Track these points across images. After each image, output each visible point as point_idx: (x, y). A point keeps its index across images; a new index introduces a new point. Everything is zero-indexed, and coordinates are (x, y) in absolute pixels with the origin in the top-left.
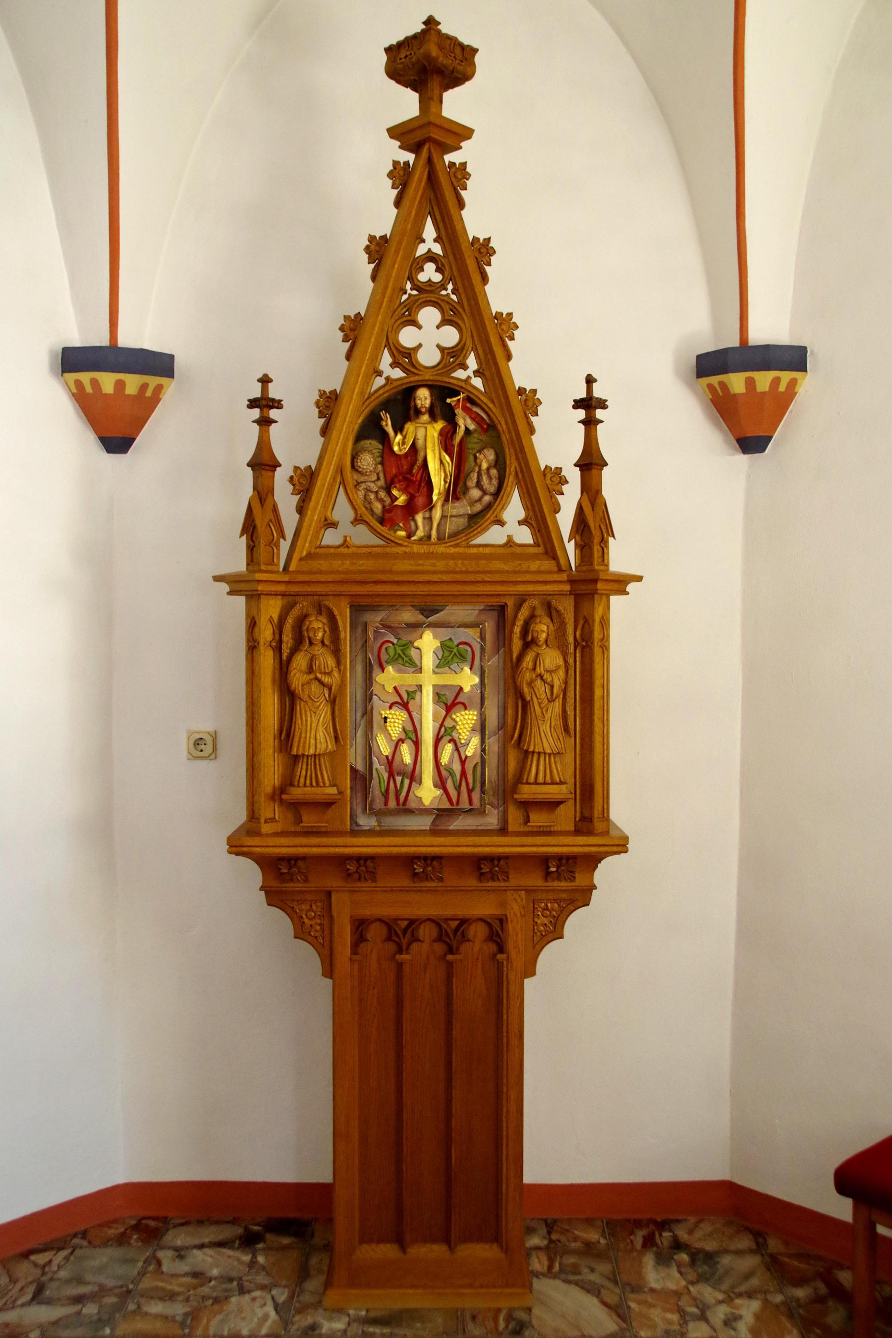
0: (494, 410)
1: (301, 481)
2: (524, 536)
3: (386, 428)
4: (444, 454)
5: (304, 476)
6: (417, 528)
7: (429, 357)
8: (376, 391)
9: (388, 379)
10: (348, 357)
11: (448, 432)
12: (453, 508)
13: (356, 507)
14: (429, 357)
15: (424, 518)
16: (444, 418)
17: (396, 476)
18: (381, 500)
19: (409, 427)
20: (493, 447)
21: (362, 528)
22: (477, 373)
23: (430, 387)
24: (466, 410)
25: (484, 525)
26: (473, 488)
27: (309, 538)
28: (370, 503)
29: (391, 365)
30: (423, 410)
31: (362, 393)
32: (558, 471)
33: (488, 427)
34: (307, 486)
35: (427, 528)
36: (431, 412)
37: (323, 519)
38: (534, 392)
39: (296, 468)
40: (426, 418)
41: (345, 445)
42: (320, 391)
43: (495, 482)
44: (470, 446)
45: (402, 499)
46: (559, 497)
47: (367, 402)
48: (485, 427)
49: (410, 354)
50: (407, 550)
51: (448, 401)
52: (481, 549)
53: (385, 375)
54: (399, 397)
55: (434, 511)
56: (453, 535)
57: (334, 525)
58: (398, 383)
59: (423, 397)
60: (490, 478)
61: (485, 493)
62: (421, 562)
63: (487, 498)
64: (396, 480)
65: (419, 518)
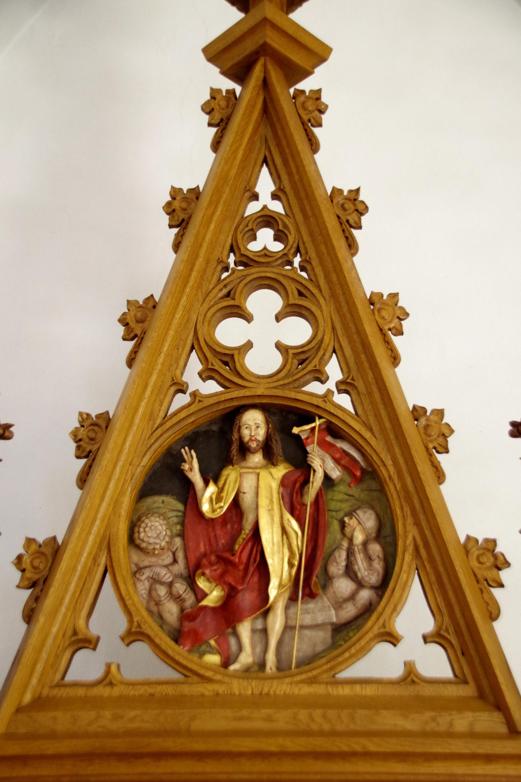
0: (373, 442)
1: (36, 563)
2: (435, 664)
3: (190, 475)
4: (288, 516)
5: (43, 554)
6: (240, 648)
7: (262, 362)
8: (175, 414)
9: (194, 395)
10: (130, 362)
12: (307, 612)
13: (132, 609)
14: (262, 362)
15: (254, 631)
16: (289, 460)
17: (205, 555)
18: (178, 599)
19: (230, 474)
20: (373, 508)
21: (141, 648)
22: (344, 387)
23: (264, 408)
24: (323, 445)
25: (363, 642)
26: (339, 576)
27: (39, 668)
28: (157, 604)
29: (200, 374)
30: (254, 445)
31: (151, 416)
32: (490, 546)
33: (364, 473)
34: (45, 573)
35: (258, 650)
37: (70, 632)
38: (440, 413)
39: (30, 541)
40: (257, 458)
41: (116, 503)
42: (81, 414)
43: (378, 566)
44: (333, 505)
45: (214, 596)
46: (496, 592)
47: (159, 431)
48: (358, 474)
49: (232, 356)
50: (221, 689)
51: (296, 430)
52: (358, 688)
53: (190, 390)
54: (215, 428)
55: (271, 617)
56: (306, 662)
57: (90, 643)
58: (212, 401)
59: (254, 425)
60: (369, 558)
61: (360, 584)
62: (245, 712)
63: (365, 595)
64: (205, 561)
65: (245, 629)
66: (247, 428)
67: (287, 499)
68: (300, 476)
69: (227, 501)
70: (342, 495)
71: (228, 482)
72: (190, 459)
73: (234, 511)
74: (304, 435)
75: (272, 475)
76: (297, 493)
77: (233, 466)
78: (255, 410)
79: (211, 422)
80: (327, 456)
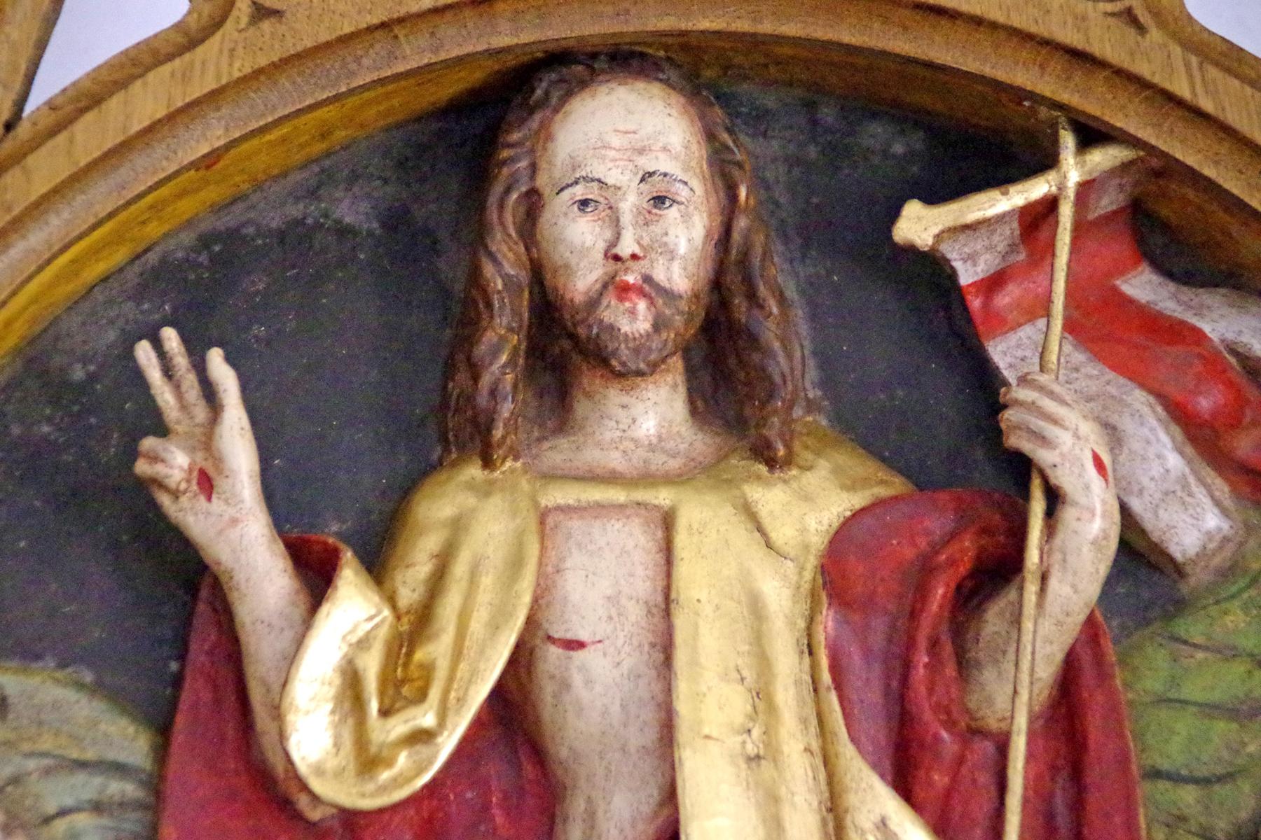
3: (196, 519)
11: (926, 569)
19: (472, 520)
24: (1105, 326)
30: (633, 321)
36: (721, 357)
40: (650, 416)
51: (918, 225)
54: (353, 210)
66: (584, 203)
67: (870, 687)
68: (953, 536)
69: (461, 701)
70: (1240, 667)
71: (460, 569)
72: (201, 413)
73: (496, 771)
74: (971, 258)
75: (760, 529)
76: (934, 643)
77: (488, 463)
78: (640, 85)
79: (324, 174)
80: (1139, 398)
